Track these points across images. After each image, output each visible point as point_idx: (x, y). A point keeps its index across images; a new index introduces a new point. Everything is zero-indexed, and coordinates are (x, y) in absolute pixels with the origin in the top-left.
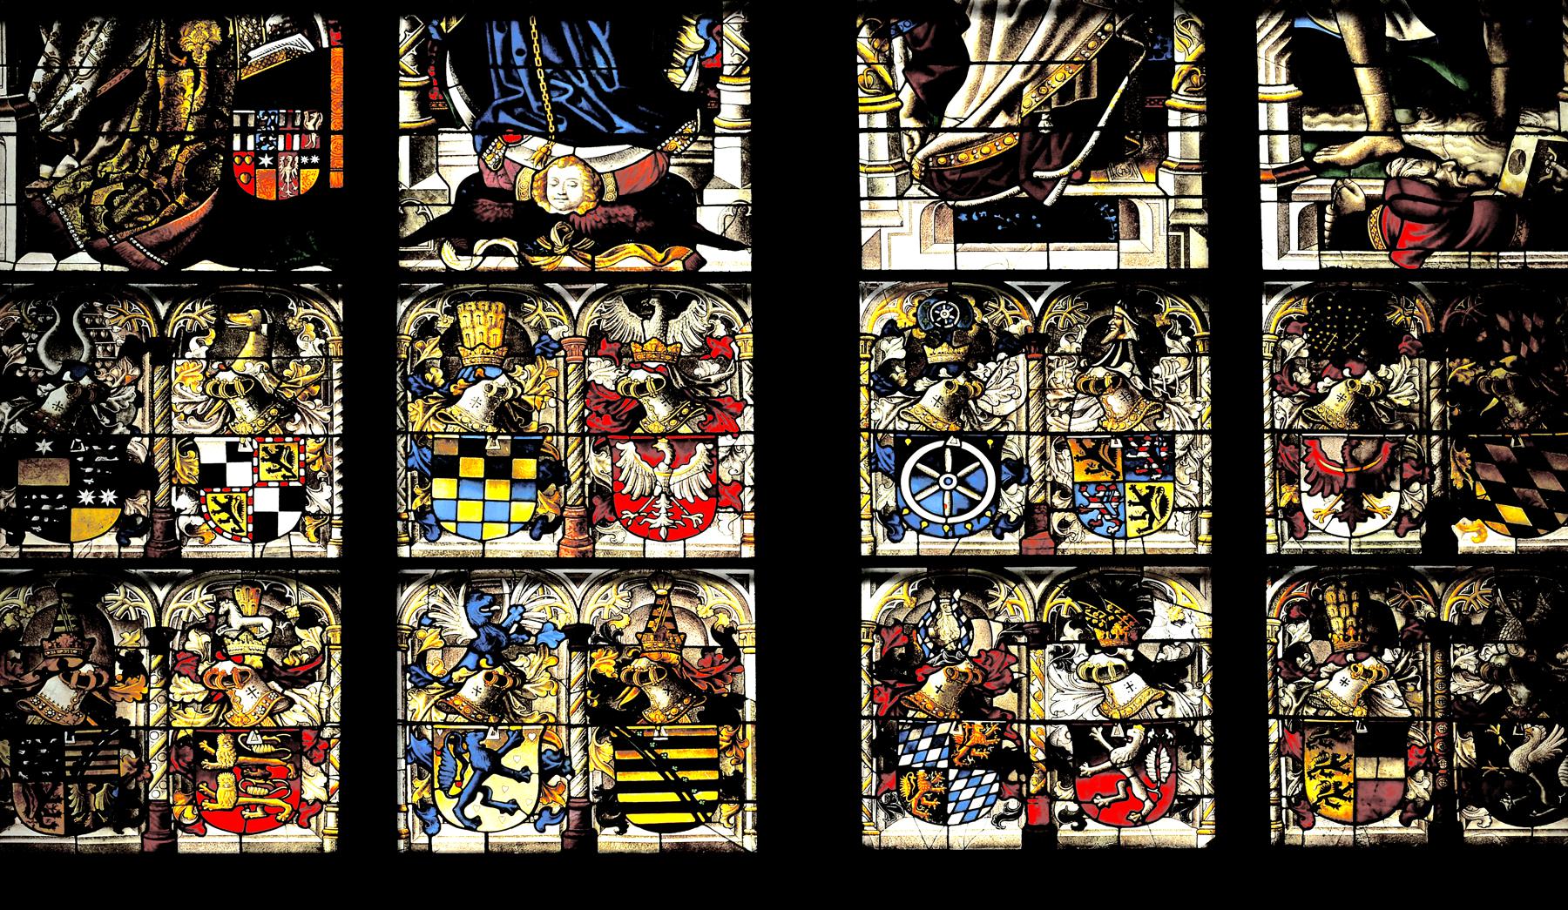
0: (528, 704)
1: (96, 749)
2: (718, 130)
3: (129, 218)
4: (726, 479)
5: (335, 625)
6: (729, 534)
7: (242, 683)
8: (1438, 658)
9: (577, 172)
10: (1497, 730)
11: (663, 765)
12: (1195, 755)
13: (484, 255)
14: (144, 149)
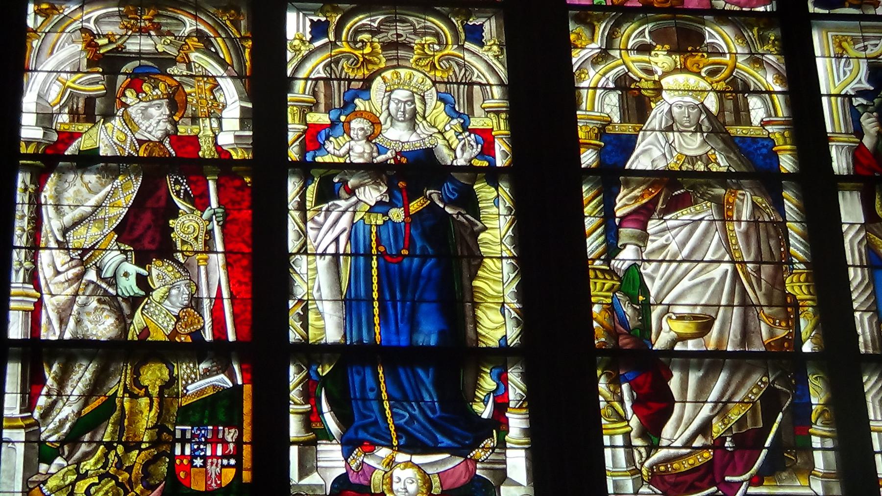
2: (508, 445)
14: (113, 453)
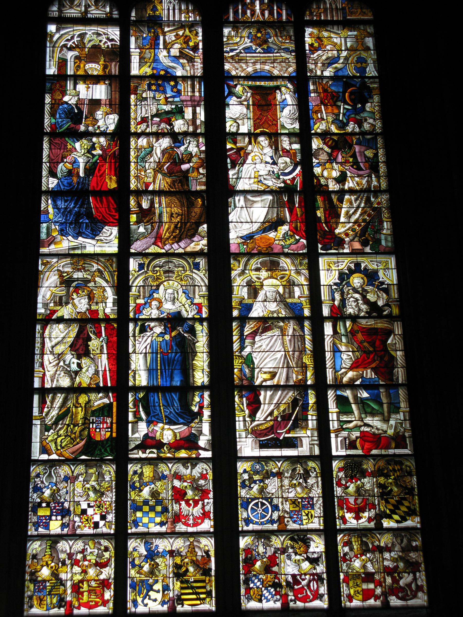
0: (159, 571)
1: (54, 586)
3: (66, 445)
4: (207, 511)
5: (113, 551)
6: (207, 525)
7: (90, 568)
8: (381, 555)
9: (170, 432)
10: (396, 575)
11: (192, 588)
12: (323, 583)
13: (149, 453)
